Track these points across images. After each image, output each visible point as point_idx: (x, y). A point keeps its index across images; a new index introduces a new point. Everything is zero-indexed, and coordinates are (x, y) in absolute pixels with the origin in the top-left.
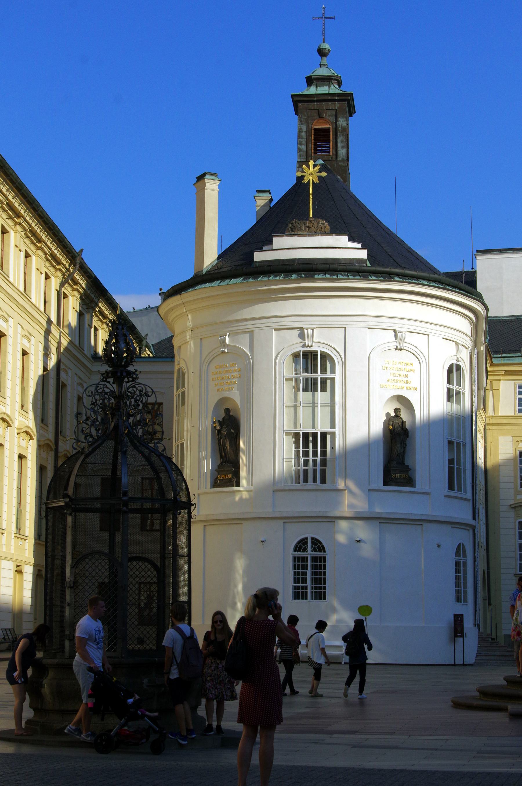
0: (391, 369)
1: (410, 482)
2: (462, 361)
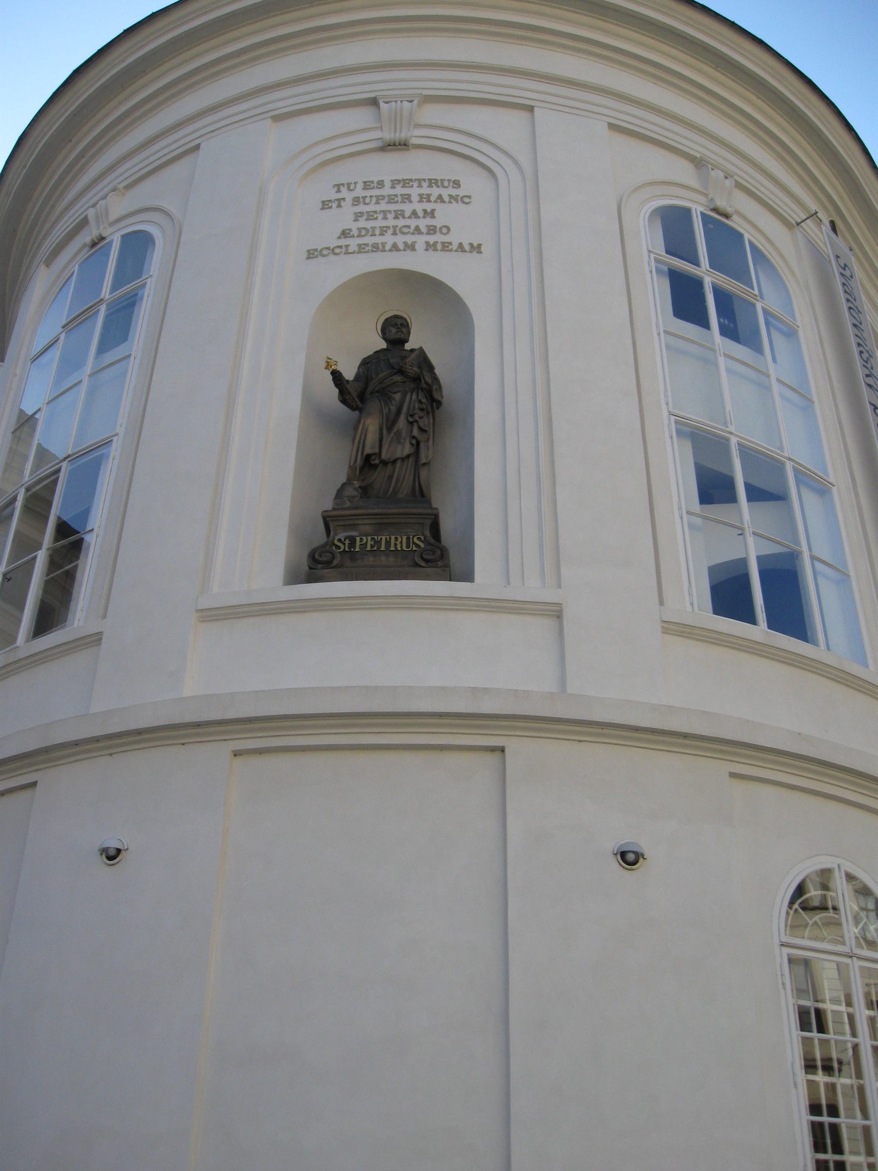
0: (356, 201)
1: (427, 561)
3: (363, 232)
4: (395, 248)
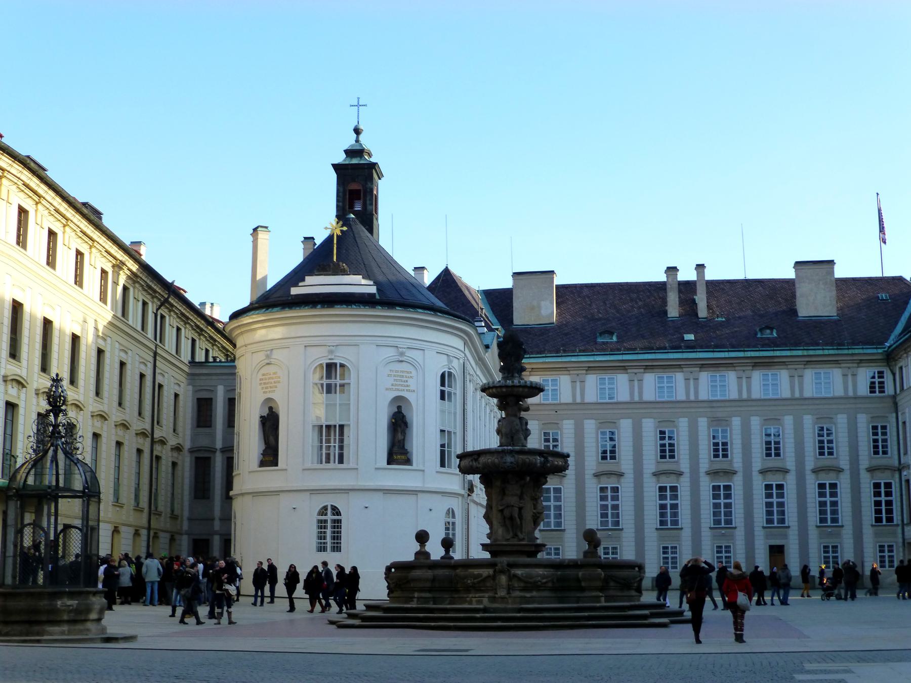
2: (454, 369)
3: (396, 385)
4: (401, 391)
